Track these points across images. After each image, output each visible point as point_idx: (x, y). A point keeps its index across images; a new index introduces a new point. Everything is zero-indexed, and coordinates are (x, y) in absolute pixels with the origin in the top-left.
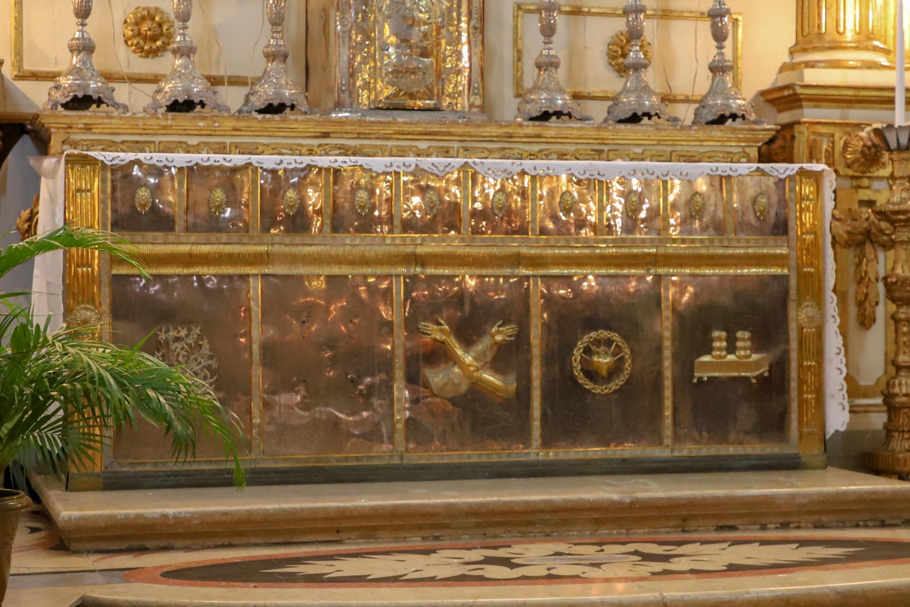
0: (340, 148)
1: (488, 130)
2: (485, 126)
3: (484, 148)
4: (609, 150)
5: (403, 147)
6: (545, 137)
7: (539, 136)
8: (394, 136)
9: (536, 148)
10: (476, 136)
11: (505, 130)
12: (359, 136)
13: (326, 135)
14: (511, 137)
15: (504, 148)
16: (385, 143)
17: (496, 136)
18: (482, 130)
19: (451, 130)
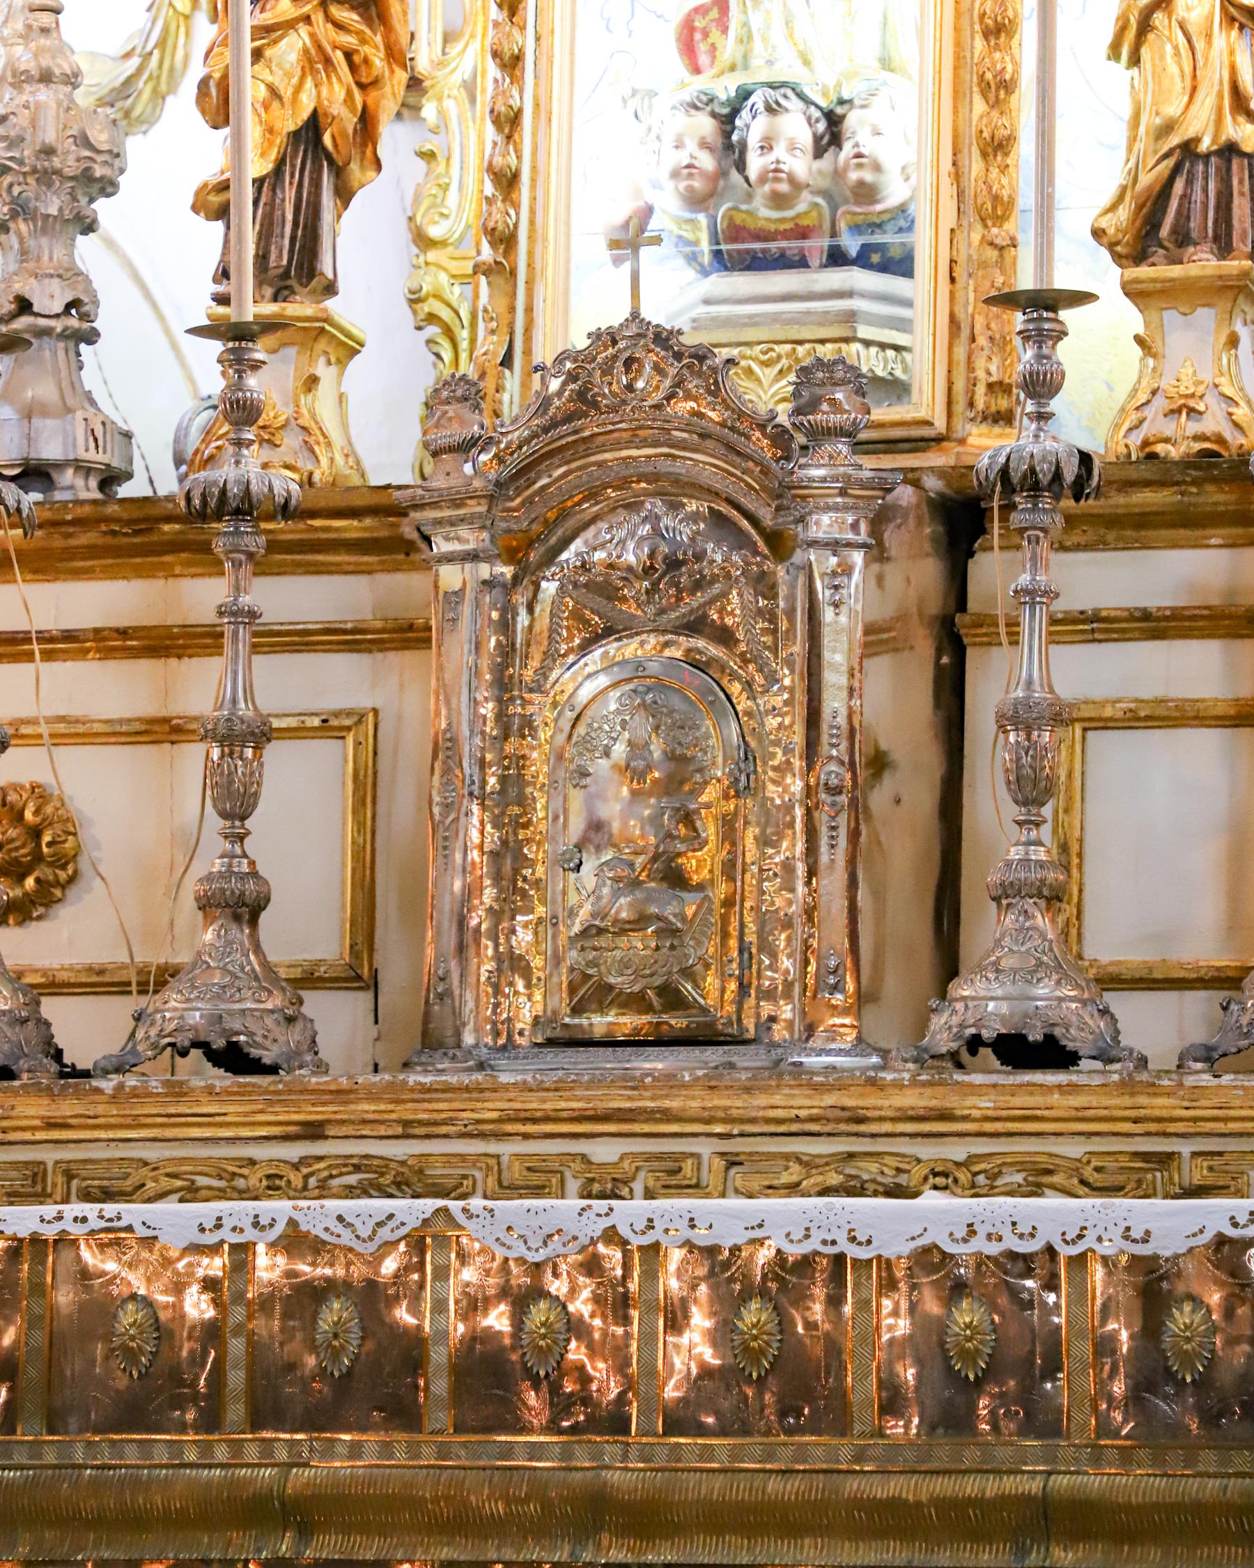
0: (357, 1168)
1: (777, 1099)
2: (764, 1090)
3: (787, 1157)
4: (1195, 1154)
5: (543, 1158)
6: (966, 1118)
7: (945, 1116)
8: (509, 1128)
9: (957, 1151)
10: (753, 1121)
11: (829, 1100)
12: (408, 1129)
13: (313, 1131)
14: (861, 1120)
15: (851, 1156)
16: (493, 1147)
17: (812, 1119)
18: (762, 1100)
19: (667, 1104)
